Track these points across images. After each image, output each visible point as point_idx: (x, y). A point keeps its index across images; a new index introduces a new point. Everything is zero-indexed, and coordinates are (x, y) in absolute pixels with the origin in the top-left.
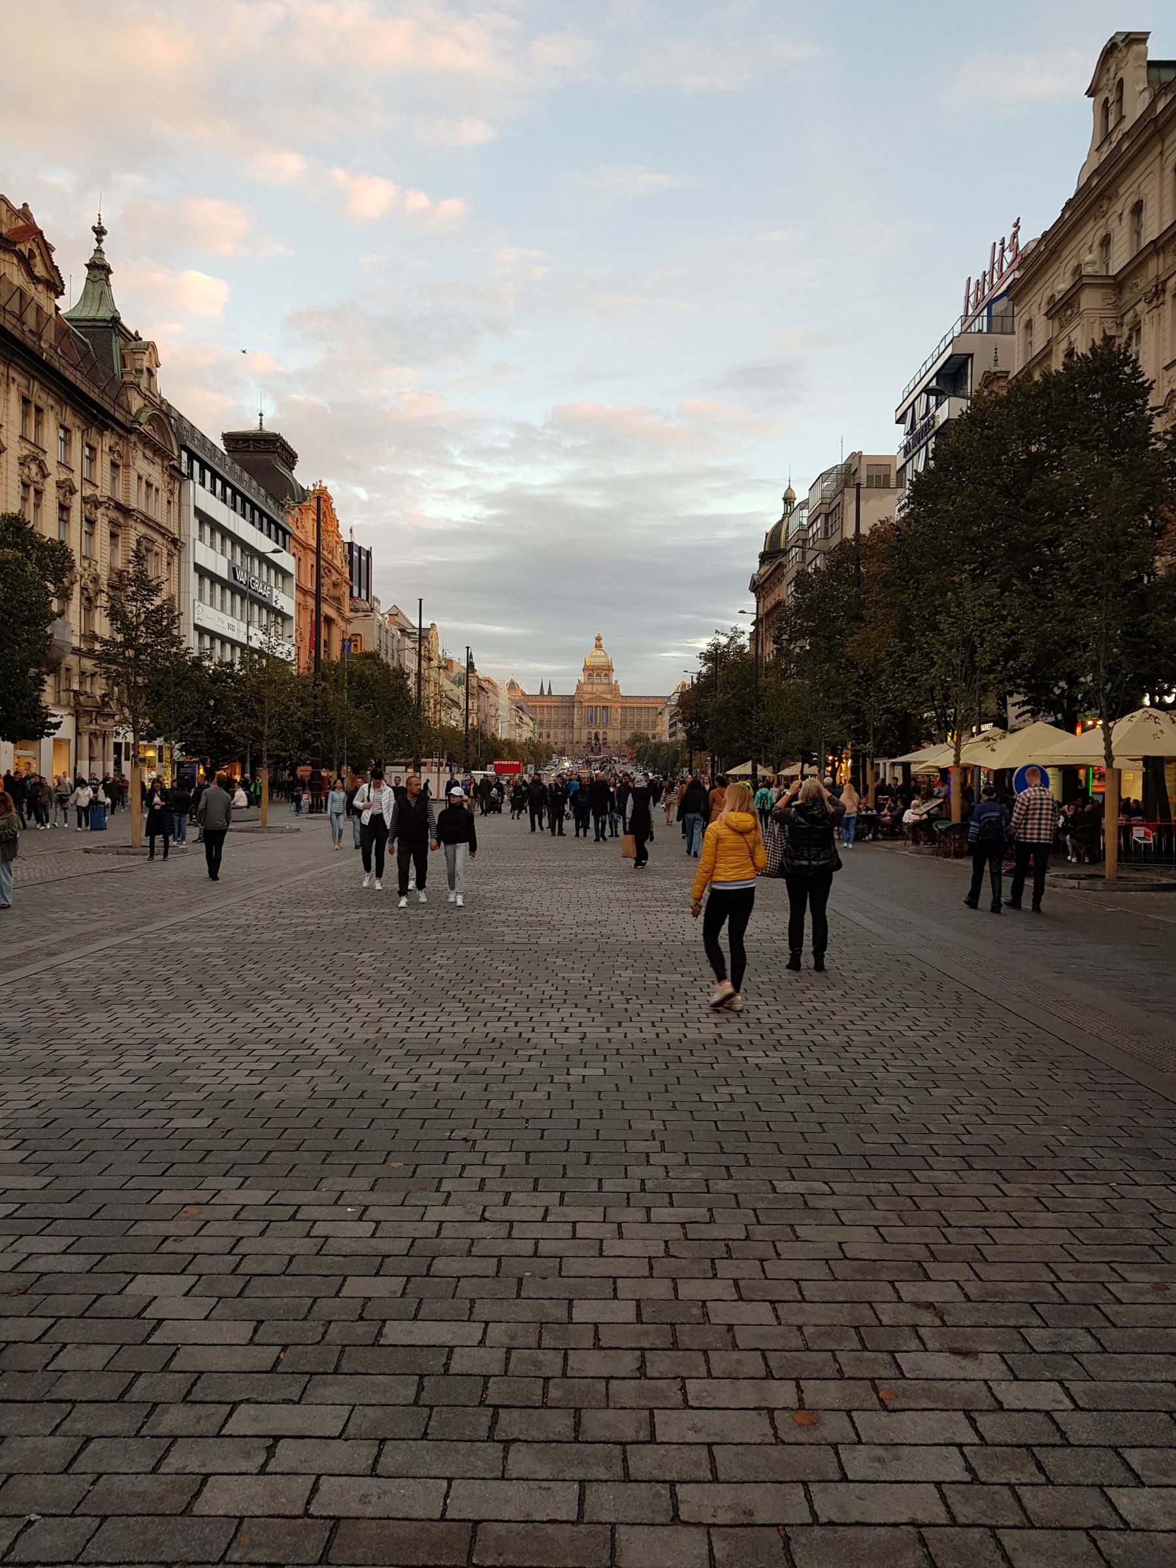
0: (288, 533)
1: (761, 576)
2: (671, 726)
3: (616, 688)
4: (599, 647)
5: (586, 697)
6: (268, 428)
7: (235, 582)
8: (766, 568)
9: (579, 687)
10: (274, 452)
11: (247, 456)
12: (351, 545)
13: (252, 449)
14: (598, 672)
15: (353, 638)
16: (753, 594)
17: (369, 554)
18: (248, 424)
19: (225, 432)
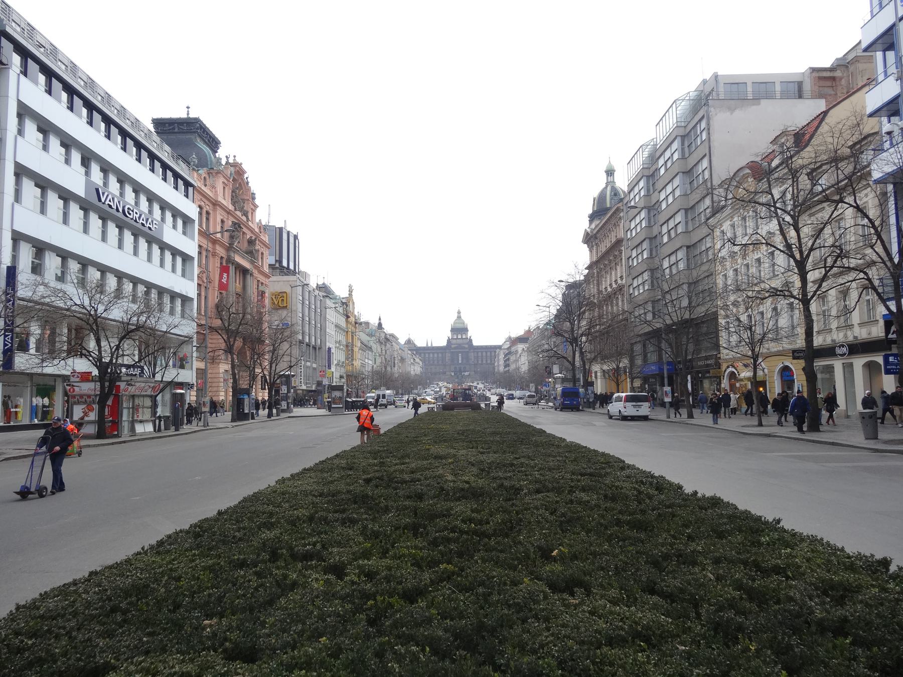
0: (192, 185)
1: (592, 230)
2: (505, 361)
3: (471, 341)
4: (459, 317)
5: (453, 346)
6: (192, 116)
7: (100, 204)
8: (596, 222)
9: (449, 341)
10: (195, 132)
11: (173, 137)
12: (281, 229)
13: (176, 130)
14: (459, 329)
15: (281, 295)
16: (586, 245)
17: (296, 237)
18: (177, 112)
19: (155, 117)
